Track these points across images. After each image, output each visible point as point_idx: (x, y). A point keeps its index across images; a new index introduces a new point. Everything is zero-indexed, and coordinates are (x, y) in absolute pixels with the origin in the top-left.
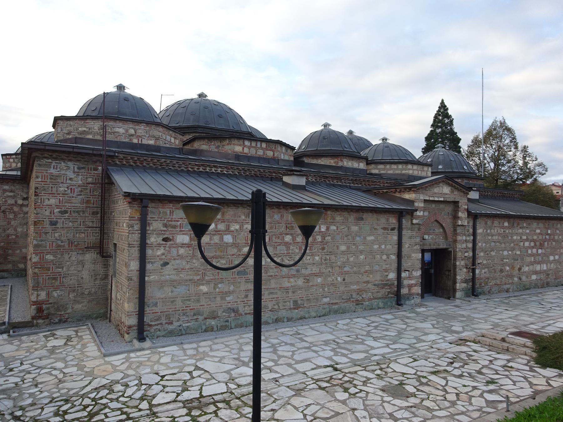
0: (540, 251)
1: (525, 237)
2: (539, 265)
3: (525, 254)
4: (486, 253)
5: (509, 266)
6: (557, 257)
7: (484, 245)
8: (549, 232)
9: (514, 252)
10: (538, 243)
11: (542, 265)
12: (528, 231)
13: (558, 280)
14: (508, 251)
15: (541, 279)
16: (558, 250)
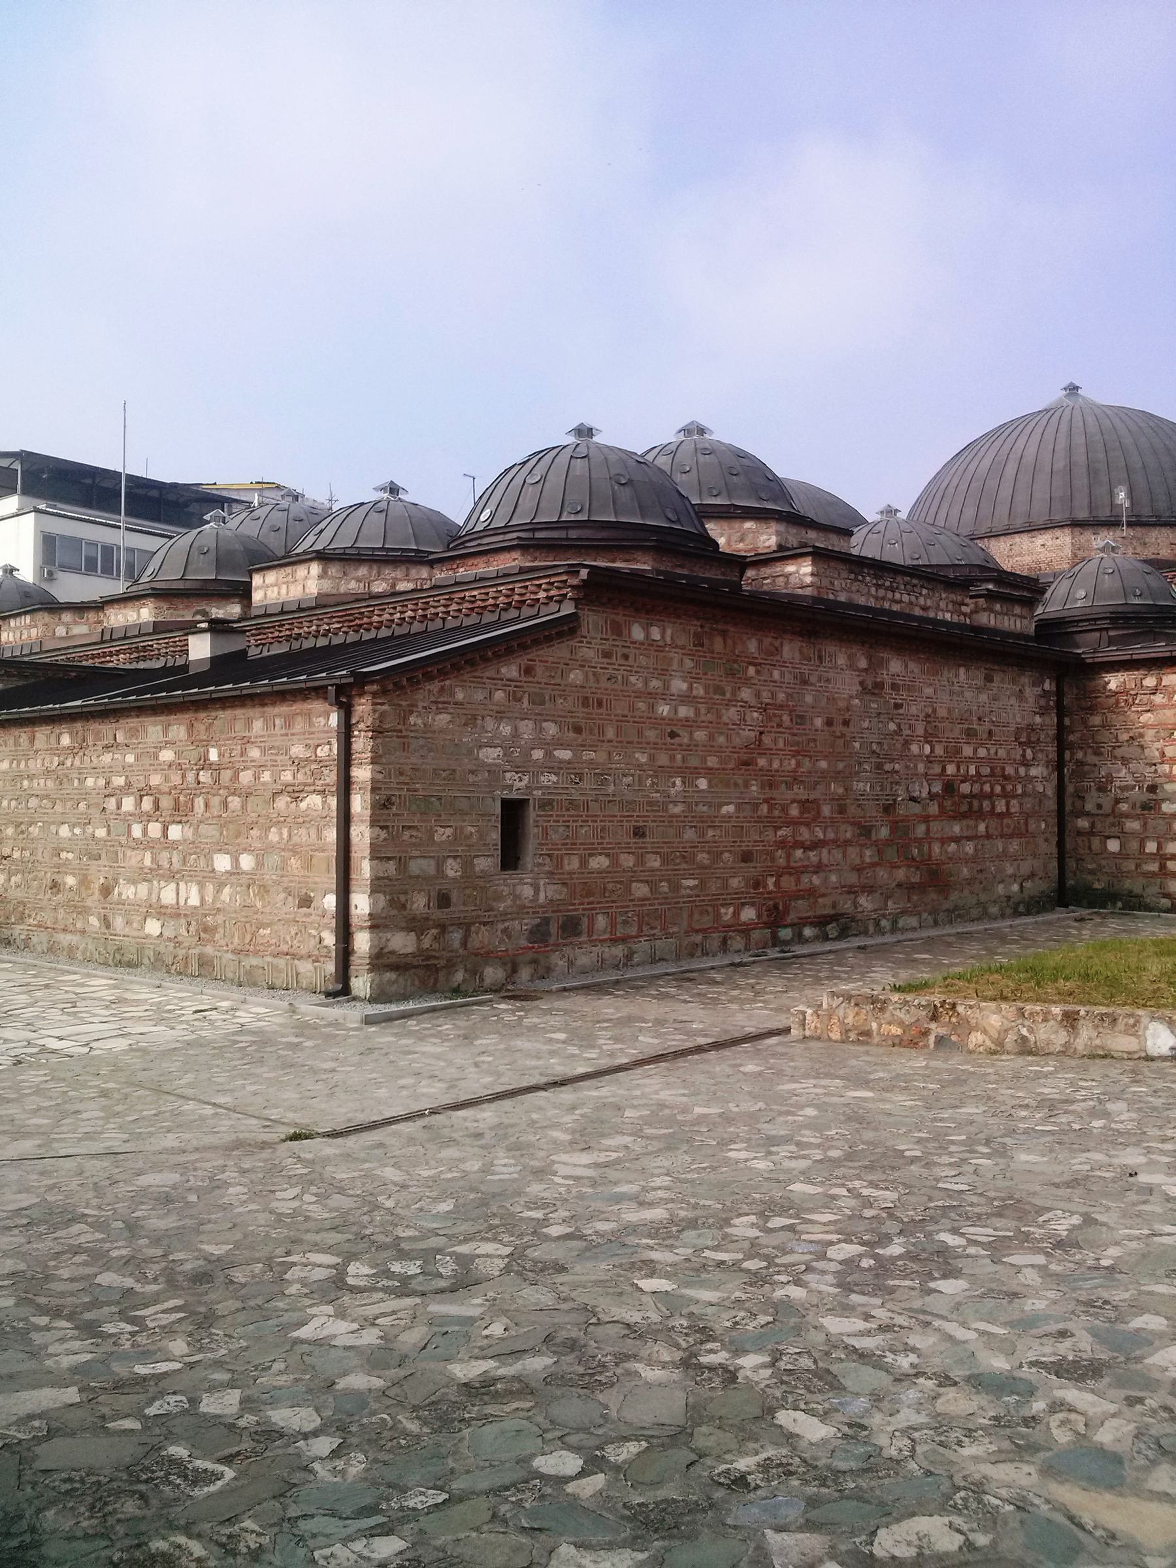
0: (175, 832)
1: (119, 781)
2: (173, 886)
3: (123, 839)
4: (19, 830)
5: (74, 875)
6: (247, 862)
7: (13, 803)
8: (213, 755)
9: (90, 829)
10: (166, 803)
11: (182, 885)
12: (130, 758)
13: (254, 961)
14: (73, 826)
15: (176, 941)
16: (255, 833)
